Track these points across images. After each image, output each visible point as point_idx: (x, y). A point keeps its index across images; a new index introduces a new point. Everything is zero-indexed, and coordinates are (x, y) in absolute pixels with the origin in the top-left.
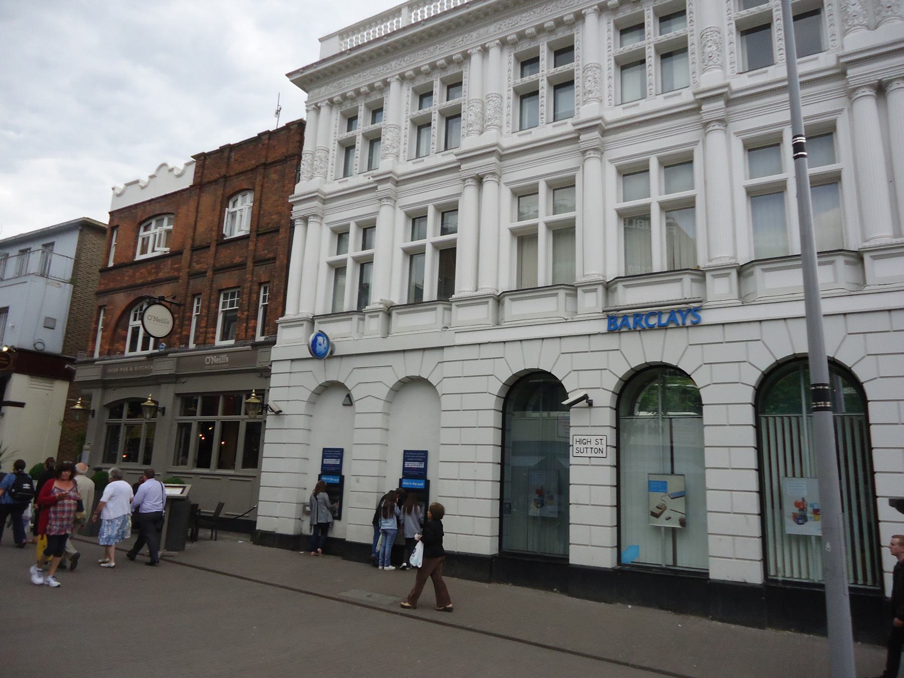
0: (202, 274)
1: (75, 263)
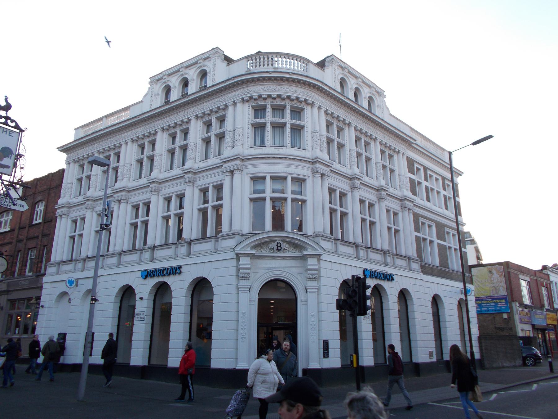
0: (21, 241)
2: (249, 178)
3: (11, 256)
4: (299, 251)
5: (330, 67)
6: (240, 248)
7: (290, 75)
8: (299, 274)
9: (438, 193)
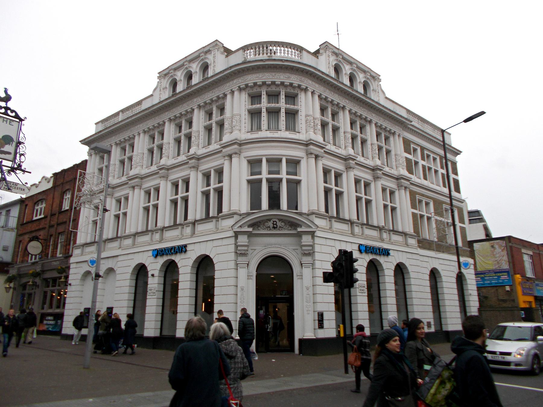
0: (53, 226)
1: (18, 219)
3: (45, 240)
4: (294, 229)
5: (324, 54)
6: (238, 226)
7: (283, 62)
8: (295, 250)
9: (436, 171)
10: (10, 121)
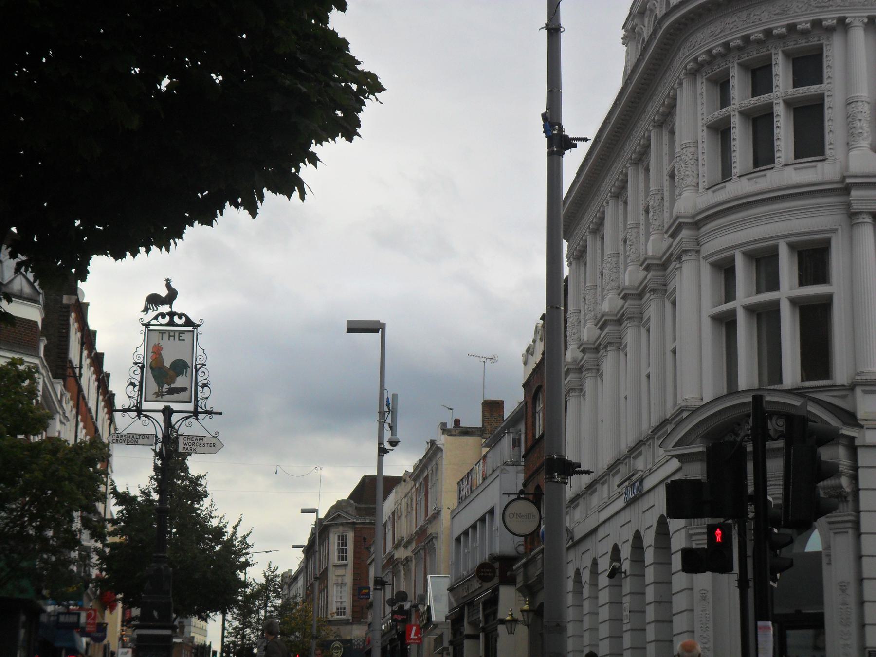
2: (708, 266)
10: (179, 334)
